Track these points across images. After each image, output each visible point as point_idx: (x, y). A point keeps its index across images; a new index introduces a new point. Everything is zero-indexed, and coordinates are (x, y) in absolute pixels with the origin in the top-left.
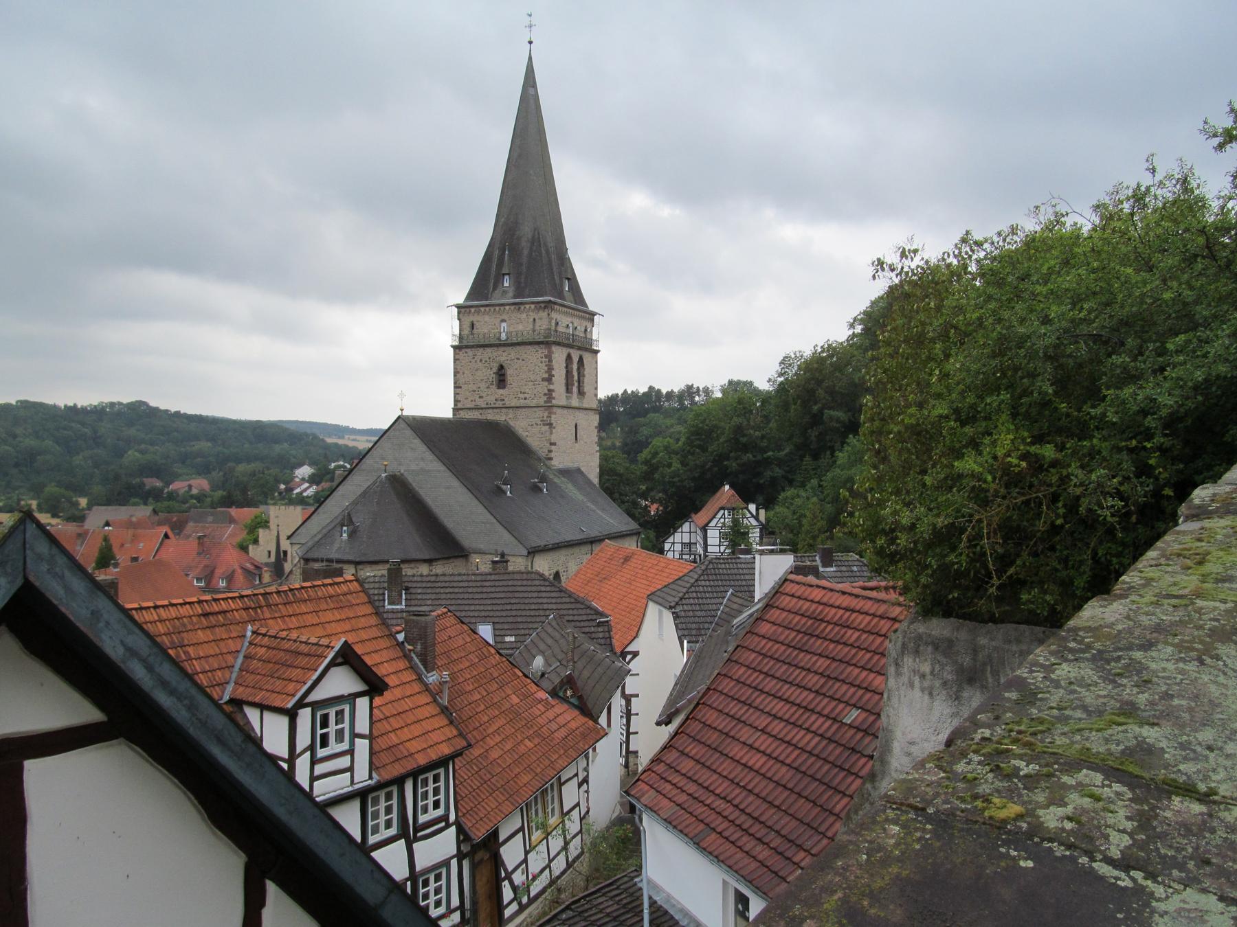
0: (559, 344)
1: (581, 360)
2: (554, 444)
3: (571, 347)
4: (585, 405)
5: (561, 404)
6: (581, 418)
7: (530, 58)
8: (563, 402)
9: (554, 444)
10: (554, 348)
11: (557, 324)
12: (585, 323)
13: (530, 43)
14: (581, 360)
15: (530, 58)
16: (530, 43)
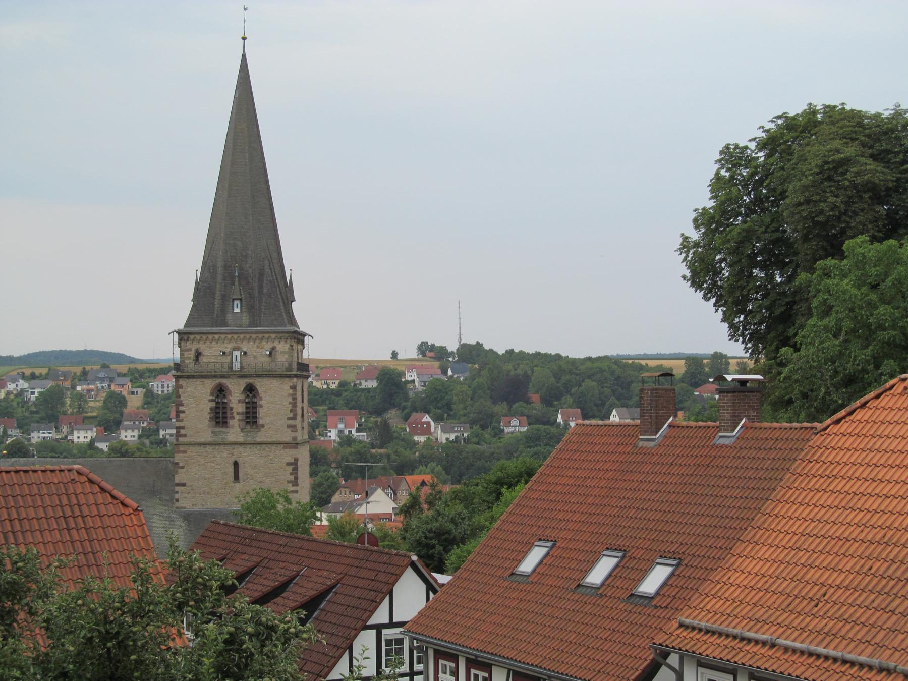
0: (193, 377)
1: (250, 390)
2: (184, 485)
3: (223, 377)
4: (258, 440)
5: (202, 440)
6: (249, 458)
7: (244, 57)
8: (207, 437)
9: (184, 485)
10: (182, 382)
11: (198, 354)
12: (269, 345)
13: (244, 39)
14: (250, 390)
15: (244, 57)
16: (244, 39)
